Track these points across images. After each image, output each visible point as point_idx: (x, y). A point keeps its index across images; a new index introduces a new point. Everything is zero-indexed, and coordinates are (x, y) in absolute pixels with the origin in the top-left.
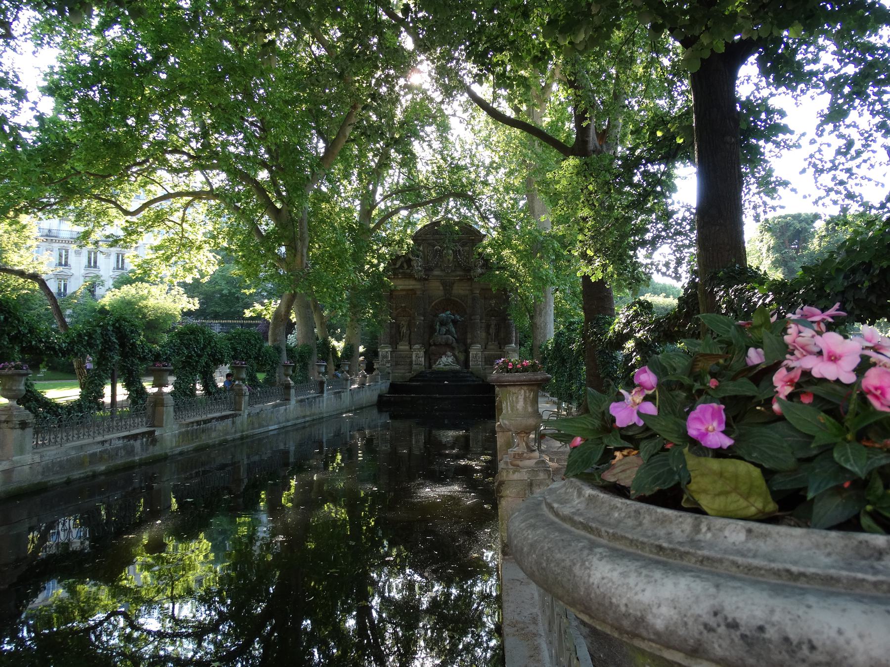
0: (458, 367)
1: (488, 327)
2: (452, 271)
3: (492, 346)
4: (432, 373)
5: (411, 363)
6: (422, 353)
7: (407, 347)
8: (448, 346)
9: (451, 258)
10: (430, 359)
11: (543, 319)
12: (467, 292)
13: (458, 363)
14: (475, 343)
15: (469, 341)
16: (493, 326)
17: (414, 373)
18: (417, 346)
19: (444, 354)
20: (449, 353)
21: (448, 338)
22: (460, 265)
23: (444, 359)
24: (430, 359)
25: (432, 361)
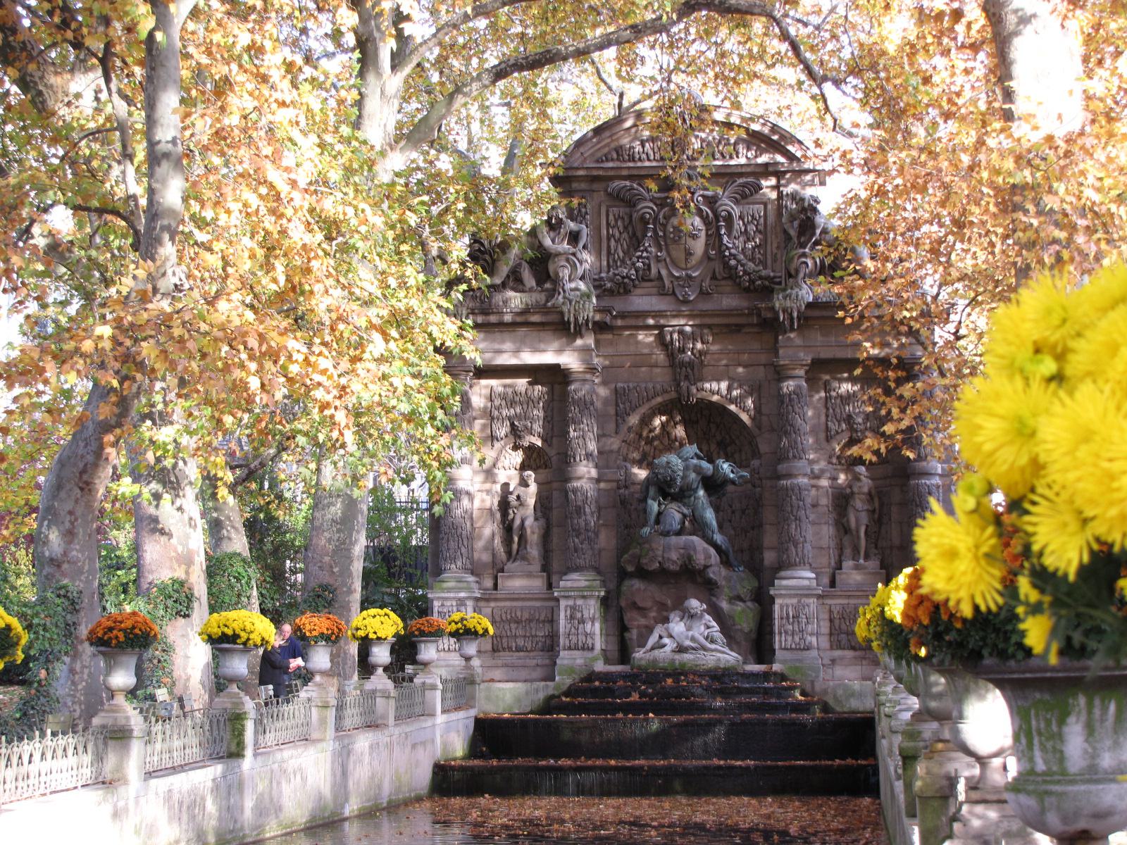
0: (726, 657)
2: (703, 294)
4: (632, 677)
5: (551, 646)
6: (592, 608)
7: (538, 583)
9: (699, 246)
10: (623, 628)
14: (790, 565)
15: (769, 557)
16: (859, 503)
17: (563, 681)
18: (577, 580)
19: (678, 604)
20: (695, 604)
22: (731, 275)
23: (678, 626)
24: (623, 628)
25: (634, 634)
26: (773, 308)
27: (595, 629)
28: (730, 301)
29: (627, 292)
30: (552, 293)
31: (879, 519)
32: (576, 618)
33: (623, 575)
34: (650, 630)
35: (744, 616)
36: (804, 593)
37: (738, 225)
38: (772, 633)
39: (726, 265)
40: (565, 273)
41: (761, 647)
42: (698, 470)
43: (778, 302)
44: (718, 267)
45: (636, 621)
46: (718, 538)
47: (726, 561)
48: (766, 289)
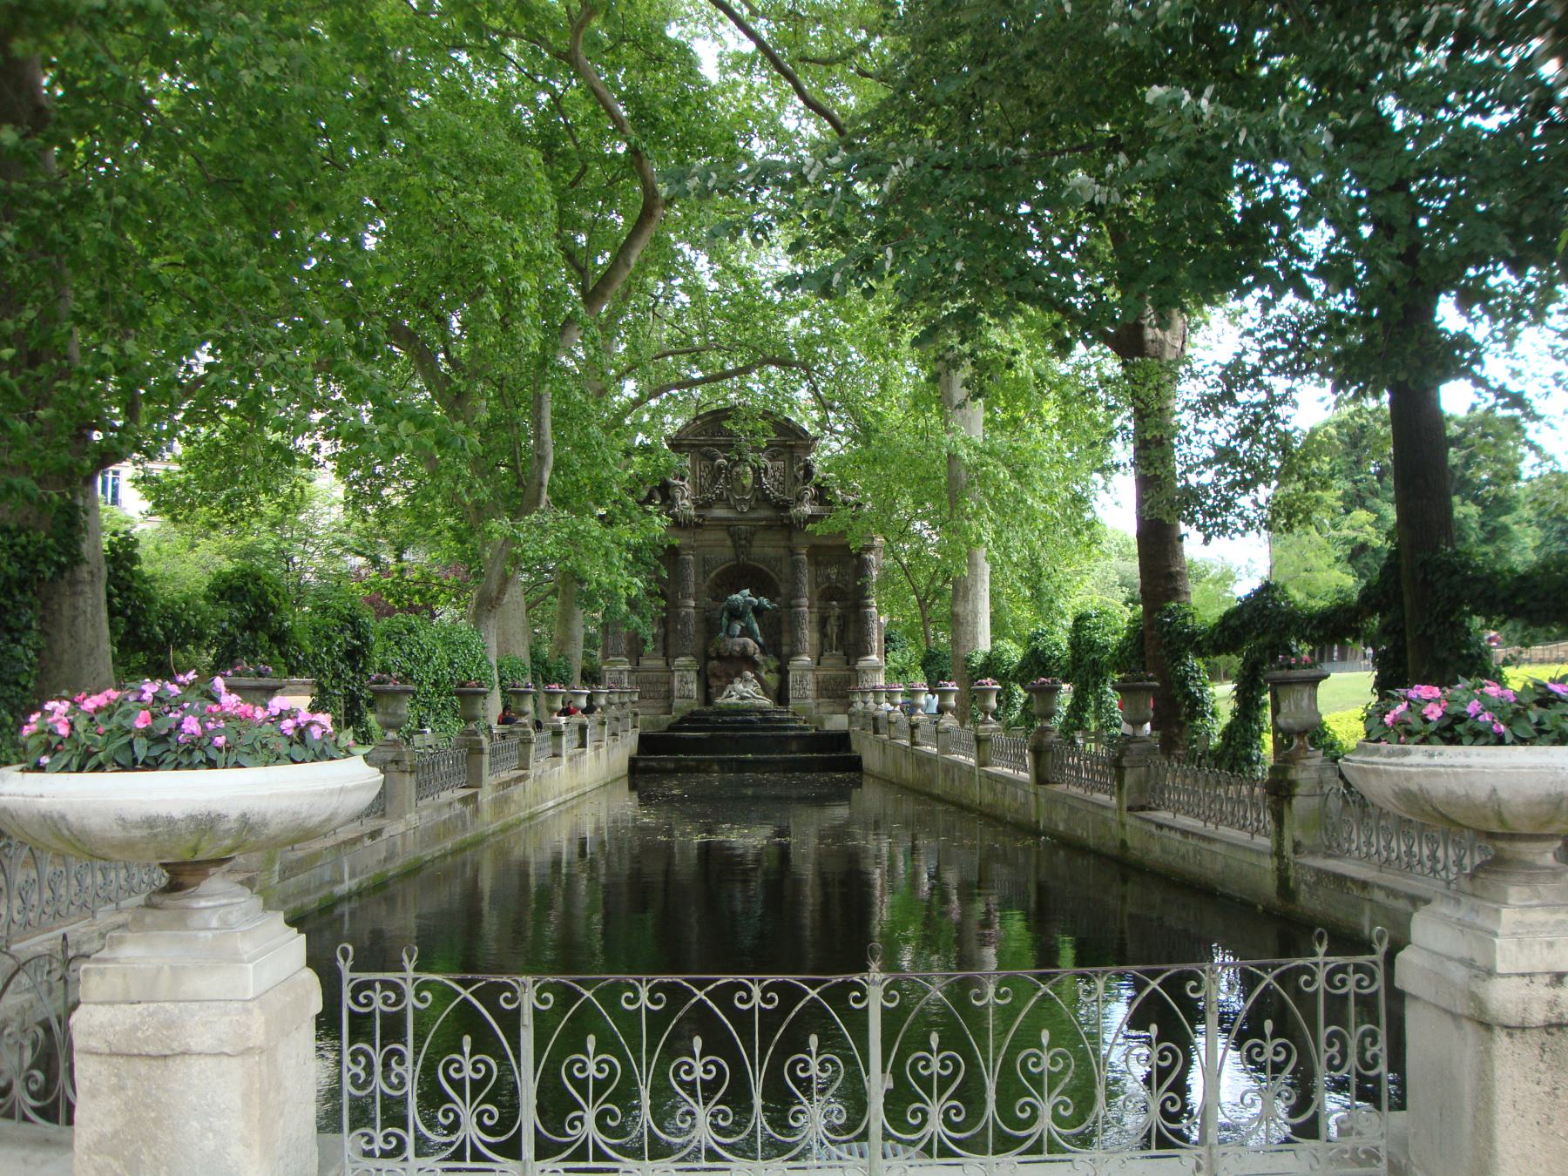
1: (823, 622)
2: (752, 509)
3: (833, 660)
5: (669, 695)
6: (692, 676)
7: (660, 663)
8: (746, 660)
9: (748, 481)
11: (970, 607)
12: (782, 551)
13: (766, 694)
14: (799, 654)
15: (785, 649)
16: (832, 620)
17: (676, 716)
18: (682, 661)
19: (739, 674)
20: (749, 674)
21: (745, 647)
22: (766, 498)
25: (714, 690)
26: (790, 518)
27: (693, 687)
28: (764, 513)
29: (710, 506)
30: (672, 507)
31: (843, 629)
32: (685, 682)
33: (708, 658)
34: (723, 689)
35: (772, 680)
36: (806, 669)
37: (770, 472)
38: (787, 689)
39: (763, 491)
40: (679, 495)
41: (781, 696)
42: (751, 602)
43: (793, 512)
44: (759, 495)
45: (714, 682)
46: (760, 639)
47: (763, 652)
48: (786, 506)
